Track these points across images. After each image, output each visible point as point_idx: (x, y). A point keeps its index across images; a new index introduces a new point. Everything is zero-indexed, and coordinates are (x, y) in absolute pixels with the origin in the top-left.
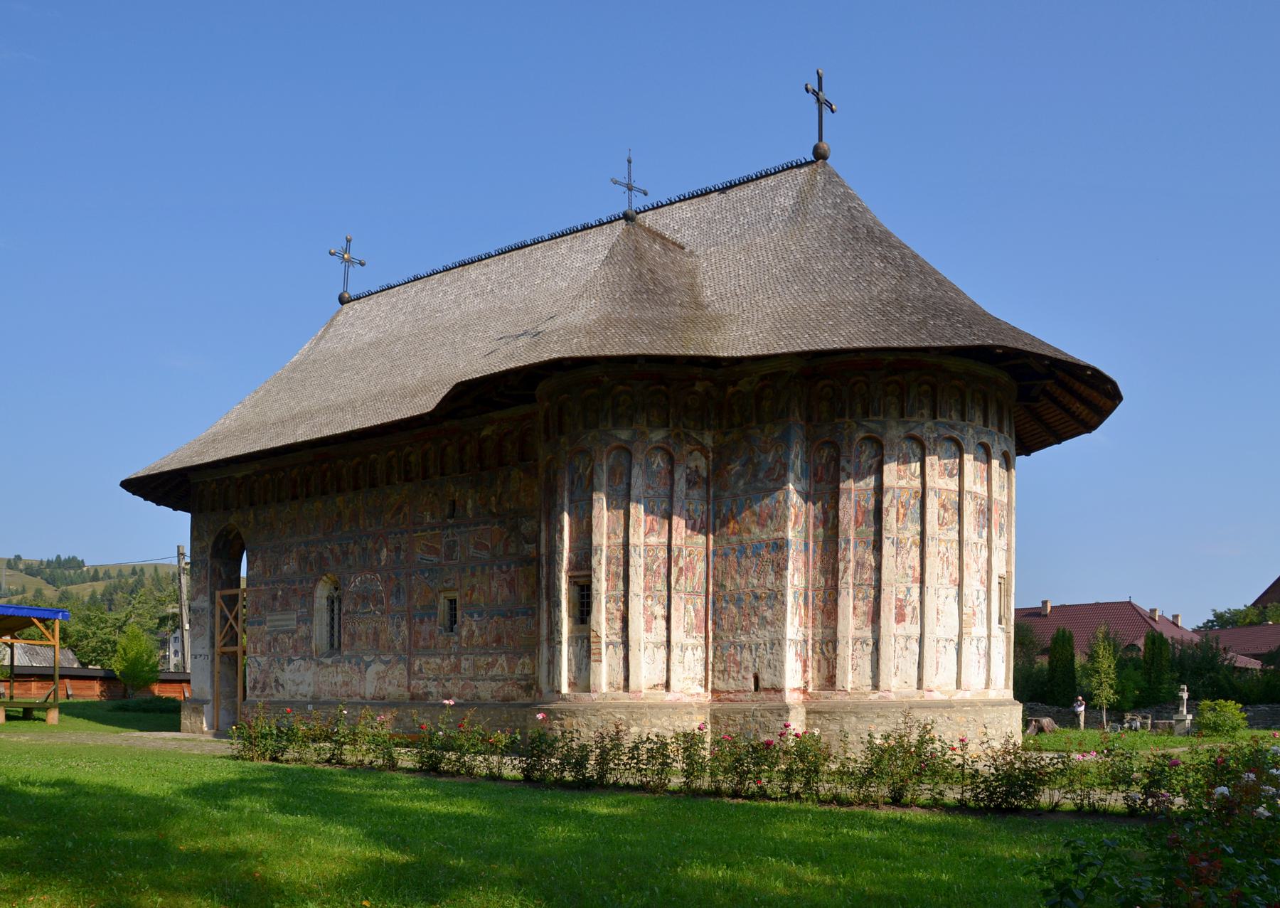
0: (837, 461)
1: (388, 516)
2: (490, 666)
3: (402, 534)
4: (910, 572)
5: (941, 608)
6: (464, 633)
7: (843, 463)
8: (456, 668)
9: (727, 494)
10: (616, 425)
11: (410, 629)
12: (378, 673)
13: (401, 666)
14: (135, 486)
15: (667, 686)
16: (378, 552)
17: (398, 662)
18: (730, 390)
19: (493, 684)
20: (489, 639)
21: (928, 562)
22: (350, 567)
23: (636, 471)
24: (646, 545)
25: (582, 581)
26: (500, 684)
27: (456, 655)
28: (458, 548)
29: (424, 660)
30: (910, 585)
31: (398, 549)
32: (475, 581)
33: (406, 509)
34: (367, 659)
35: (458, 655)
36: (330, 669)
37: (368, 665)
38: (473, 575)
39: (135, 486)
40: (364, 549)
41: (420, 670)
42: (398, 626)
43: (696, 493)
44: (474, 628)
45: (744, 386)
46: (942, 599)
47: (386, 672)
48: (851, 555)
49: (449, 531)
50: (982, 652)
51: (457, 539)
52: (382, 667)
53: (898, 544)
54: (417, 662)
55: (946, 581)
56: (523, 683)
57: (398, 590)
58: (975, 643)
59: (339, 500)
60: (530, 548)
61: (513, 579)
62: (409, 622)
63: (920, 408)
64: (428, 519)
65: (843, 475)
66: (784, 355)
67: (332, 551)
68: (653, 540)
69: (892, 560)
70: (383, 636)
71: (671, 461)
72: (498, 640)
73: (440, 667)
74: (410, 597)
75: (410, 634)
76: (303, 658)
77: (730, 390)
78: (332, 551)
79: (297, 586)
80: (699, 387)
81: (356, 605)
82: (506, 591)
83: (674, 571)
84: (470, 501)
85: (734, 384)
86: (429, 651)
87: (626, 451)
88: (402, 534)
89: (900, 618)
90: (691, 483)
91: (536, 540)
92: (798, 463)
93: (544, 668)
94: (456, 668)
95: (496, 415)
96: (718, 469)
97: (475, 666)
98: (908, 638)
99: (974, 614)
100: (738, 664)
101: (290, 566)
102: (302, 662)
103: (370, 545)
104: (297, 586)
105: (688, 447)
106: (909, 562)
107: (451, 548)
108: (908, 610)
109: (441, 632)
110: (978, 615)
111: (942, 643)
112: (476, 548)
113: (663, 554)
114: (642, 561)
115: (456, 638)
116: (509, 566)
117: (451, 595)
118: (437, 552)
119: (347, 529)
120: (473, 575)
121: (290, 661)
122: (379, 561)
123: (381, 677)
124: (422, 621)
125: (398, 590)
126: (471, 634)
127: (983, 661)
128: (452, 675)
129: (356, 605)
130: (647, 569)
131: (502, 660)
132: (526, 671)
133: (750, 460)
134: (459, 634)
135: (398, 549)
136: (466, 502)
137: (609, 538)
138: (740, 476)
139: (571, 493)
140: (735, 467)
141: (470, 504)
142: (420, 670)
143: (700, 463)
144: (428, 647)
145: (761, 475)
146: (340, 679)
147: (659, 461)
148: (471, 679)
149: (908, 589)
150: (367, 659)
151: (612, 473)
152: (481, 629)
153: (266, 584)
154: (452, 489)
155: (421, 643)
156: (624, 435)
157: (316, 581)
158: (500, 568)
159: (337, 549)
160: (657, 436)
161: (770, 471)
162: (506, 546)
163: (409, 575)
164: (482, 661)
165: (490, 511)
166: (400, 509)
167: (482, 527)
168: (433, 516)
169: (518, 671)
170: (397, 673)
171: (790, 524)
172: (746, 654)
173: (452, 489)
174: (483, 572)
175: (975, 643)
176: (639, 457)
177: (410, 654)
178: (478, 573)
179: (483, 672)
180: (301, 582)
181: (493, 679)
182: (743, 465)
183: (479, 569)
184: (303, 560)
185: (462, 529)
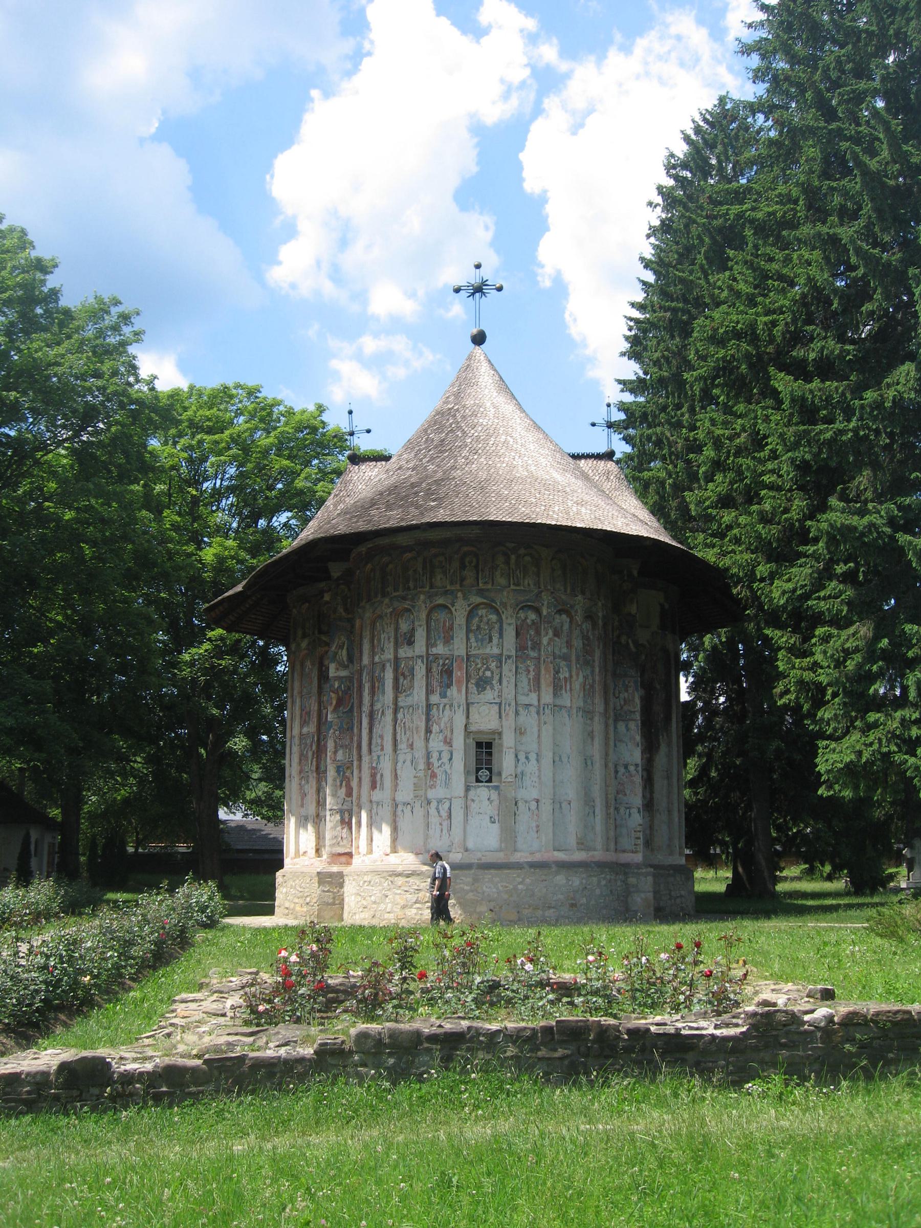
4: (379, 741)
5: (399, 772)
30: (379, 753)
46: (399, 764)
48: (355, 730)
50: (444, 814)
58: (434, 804)
68: (305, 730)
71: (313, 664)
80: (327, 597)
89: (374, 786)
92: (344, 652)
98: (378, 803)
99: (434, 775)
106: (380, 732)
110: (441, 776)
111: (400, 808)
127: (445, 823)
171: (330, 709)
175: (434, 804)
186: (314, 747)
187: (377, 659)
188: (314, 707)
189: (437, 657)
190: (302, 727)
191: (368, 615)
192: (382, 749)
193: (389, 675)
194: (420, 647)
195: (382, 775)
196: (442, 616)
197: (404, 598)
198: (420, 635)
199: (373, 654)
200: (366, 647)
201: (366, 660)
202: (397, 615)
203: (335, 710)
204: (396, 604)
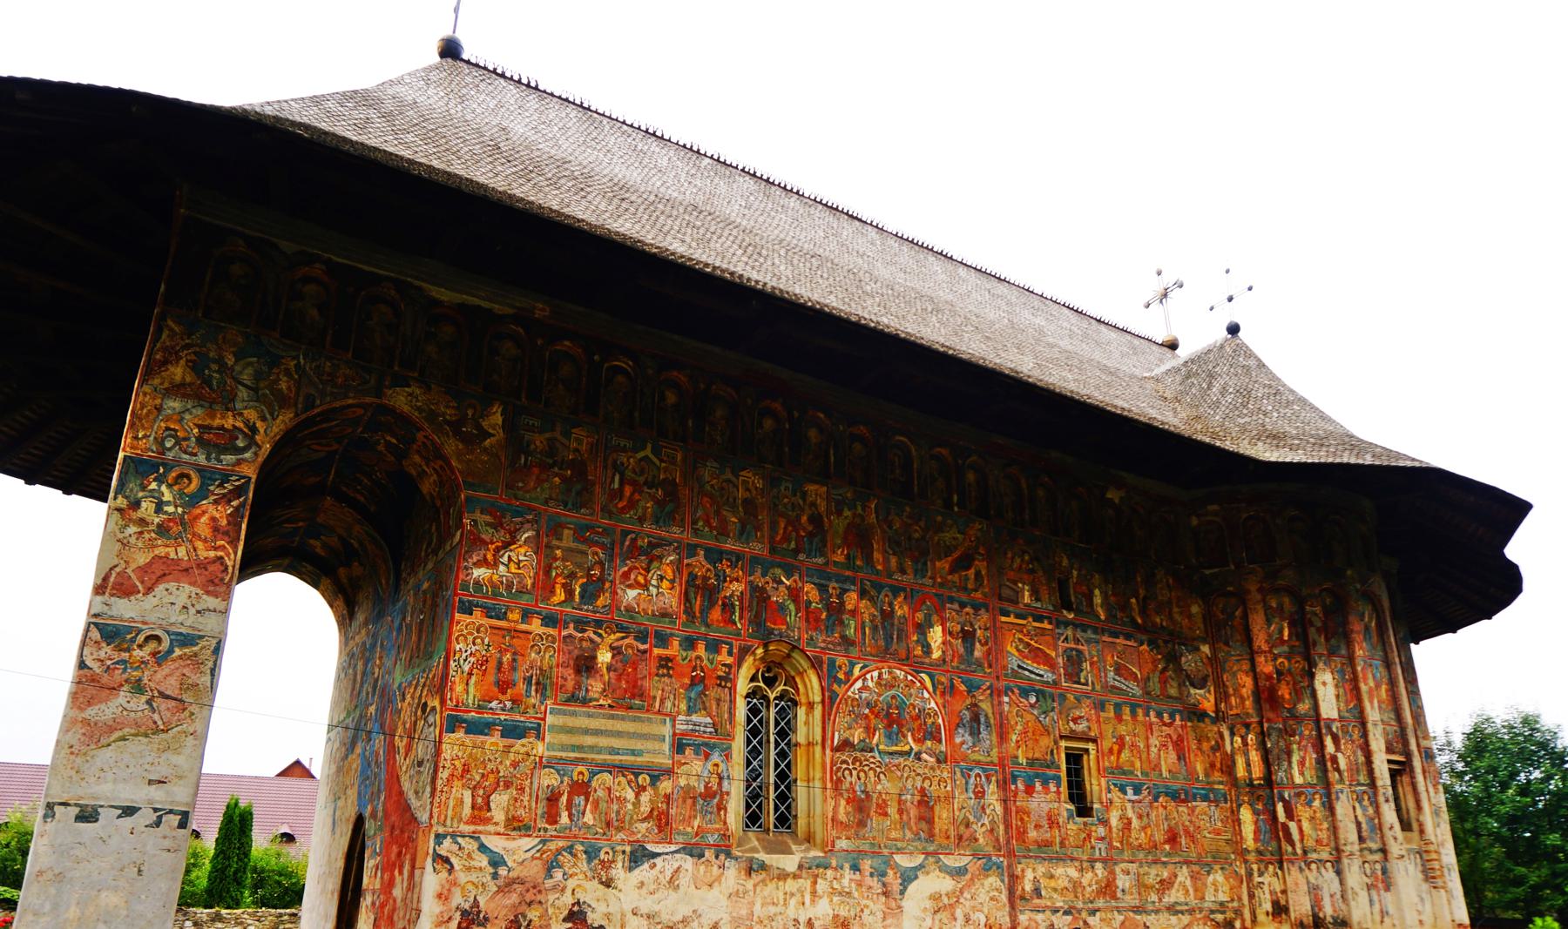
1: (943, 565)
2: (1165, 885)
3: (976, 609)
6: (1114, 822)
8: (1108, 889)
11: (1005, 801)
12: (935, 897)
13: (993, 880)
16: (922, 629)
17: (986, 870)
19: (1174, 919)
20: (1159, 837)
22: (847, 642)
26: (1186, 919)
27: (1104, 861)
28: (1086, 665)
29: (1041, 869)
32: (1122, 729)
34: (903, 861)
36: (791, 885)
37: (908, 878)
38: (1119, 718)
40: (888, 615)
41: (1037, 892)
42: (980, 794)
44: (1130, 813)
47: (957, 895)
49: (1069, 632)
51: (1084, 648)
54: (1029, 875)
56: (1219, 917)
57: (975, 718)
61: (1180, 739)
62: (1003, 785)
64: (1027, 599)
67: (794, 594)
70: (942, 815)
72: (1172, 838)
73: (1076, 885)
74: (1003, 737)
75: (1006, 810)
76: (694, 850)
78: (794, 594)
79: (674, 649)
81: (870, 731)
82: (1173, 756)
84: (1097, 592)
86: (1047, 851)
88: (976, 609)
94: (1108, 889)
97: (1142, 886)
102: (688, 863)
103: (901, 610)
104: (674, 649)
107: (1074, 662)
109: (1070, 817)
115: (1101, 831)
116: (1172, 716)
118: (1052, 665)
119: (839, 557)
120: (1119, 718)
122: (927, 650)
124: (1030, 790)
125: (975, 718)
128: (1100, 903)
129: (870, 731)
131: (1183, 875)
132: (1222, 897)
134: (1105, 822)
136: (1092, 592)
141: (1098, 600)
142: (1037, 892)
144: (1048, 844)
148: (1137, 910)
150: (903, 861)
152: (1140, 817)
153: (549, 620)
154: (1065, 562)
155: (1033, 834)
157: (745, 652)
158: (1159, 715)
159: (811, 592)
162: (1164, 682)
164: (1154, 874)
167: (1121, 641)
168: (1035, 593)
169: (1209, 897)
170: (983, 897)
173: (1065, 562)
174: (1134, 715)
177: (1011, 854)
178: (1127, 716)
179: (1154, 897)
180: (690, 643)
181: (1172, 909)
183: (1127, 710)
185: (1090, 634)
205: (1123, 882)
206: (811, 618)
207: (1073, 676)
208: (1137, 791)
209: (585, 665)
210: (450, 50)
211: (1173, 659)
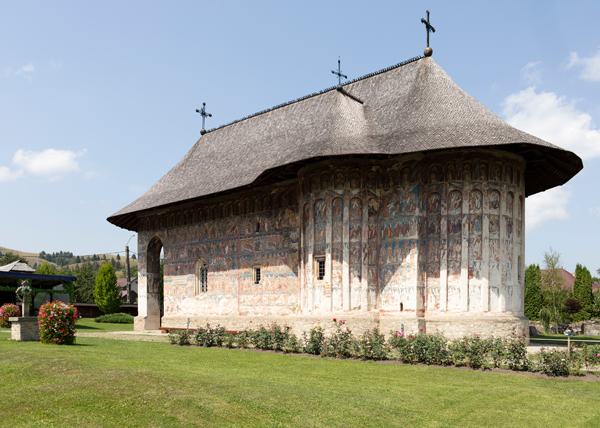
0: (440, 203)
2: (276, 299)
7: (442, 203)
8: (260, 300)
9: (387, 219)
10: (336, 187)
14: (113, 220)
15: (360, 308)
16: (224, 248)
18: (388, 169)
21: (484, 251)
23: (346, 209)
24: (350, 243)
25: (321, 260)
31: (233, 246)
33: (237, 228)
35: (261, 294)
37: (219, 299)
39: (113, 220)
43: (372, 218)
45: (395, 167)
52: (226, 300)
53: (469, 241)
55: (493, 259)
59: (206, 224)
60: (295, 246)
63: (481, 175)
65: (443, 209)
66: (415, 153)
68: (353, 240)
69: (466, 249)
70: (227, 287)
71: (361, 203)
72: (280, 287)
77: (388, 169)
80: (374, 169)
83: (363, 254)
85: (390, 167)
87: (341, 199)
90: (370, 214)
91: (298, 240)
93: (302, 300)
95: (278, 184)
96: (382, 207)
98: (475, 286)
100: (393, 298)
101: (184, 255)
105: (369, 197)
107: (258, 245)
108: (475, 273)
112: (270, 244)
113: (357, 247)
114: (347, 250)
117: (257, 267)
121: (184, 298)
123: (225, 305)
126: (267, 285)
130: (351, 253)
133: (398, 203)
135: (233, 246)
137: (333, 240)
138: (393, 210)
139: (315, 220)
140: (391, 206)
143: (375, 205)
145: (403, 209)
146: (207, 306)
147: (355, 204)
148: (268, 305)
149: (475, 263)
151: (334, 209)
156: (340, 192)
160: (355, 192)
161: (408, 207)
163: (238, 258)
164: (272, 296)
165: (276, 229)
166: (234, 228)
168: (249, 231)
172: (396, 293)
176: (347, 202)
181: (277, 305)
182: (395, 205)
184: (190, 252)
186: (366, 251)
187: (472, 212)
188: (365, 228)
189: (507, 218)
190: (350, 238)
191: (468, 188)
192: (479, 258)
193: (486, 222)
194: (504, 210)
195: (478, 272)
196: (510, 197)
197: (496, 184)
198: (503, 204)
199: (470, 209)
200: (466, 204)
201: (466, 210)
202: (490, 191)
203: (420, 231)
204: (491, 186)
205: (264, 298)
206: (205, 251)
207: (257, 249)
208: (271, 275)
209: (177, 269)
210: (203, 133)
211: (287, 236)
